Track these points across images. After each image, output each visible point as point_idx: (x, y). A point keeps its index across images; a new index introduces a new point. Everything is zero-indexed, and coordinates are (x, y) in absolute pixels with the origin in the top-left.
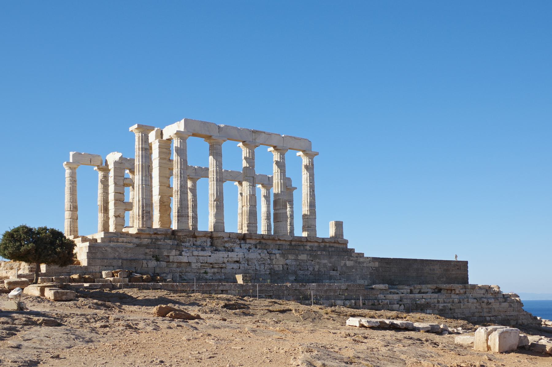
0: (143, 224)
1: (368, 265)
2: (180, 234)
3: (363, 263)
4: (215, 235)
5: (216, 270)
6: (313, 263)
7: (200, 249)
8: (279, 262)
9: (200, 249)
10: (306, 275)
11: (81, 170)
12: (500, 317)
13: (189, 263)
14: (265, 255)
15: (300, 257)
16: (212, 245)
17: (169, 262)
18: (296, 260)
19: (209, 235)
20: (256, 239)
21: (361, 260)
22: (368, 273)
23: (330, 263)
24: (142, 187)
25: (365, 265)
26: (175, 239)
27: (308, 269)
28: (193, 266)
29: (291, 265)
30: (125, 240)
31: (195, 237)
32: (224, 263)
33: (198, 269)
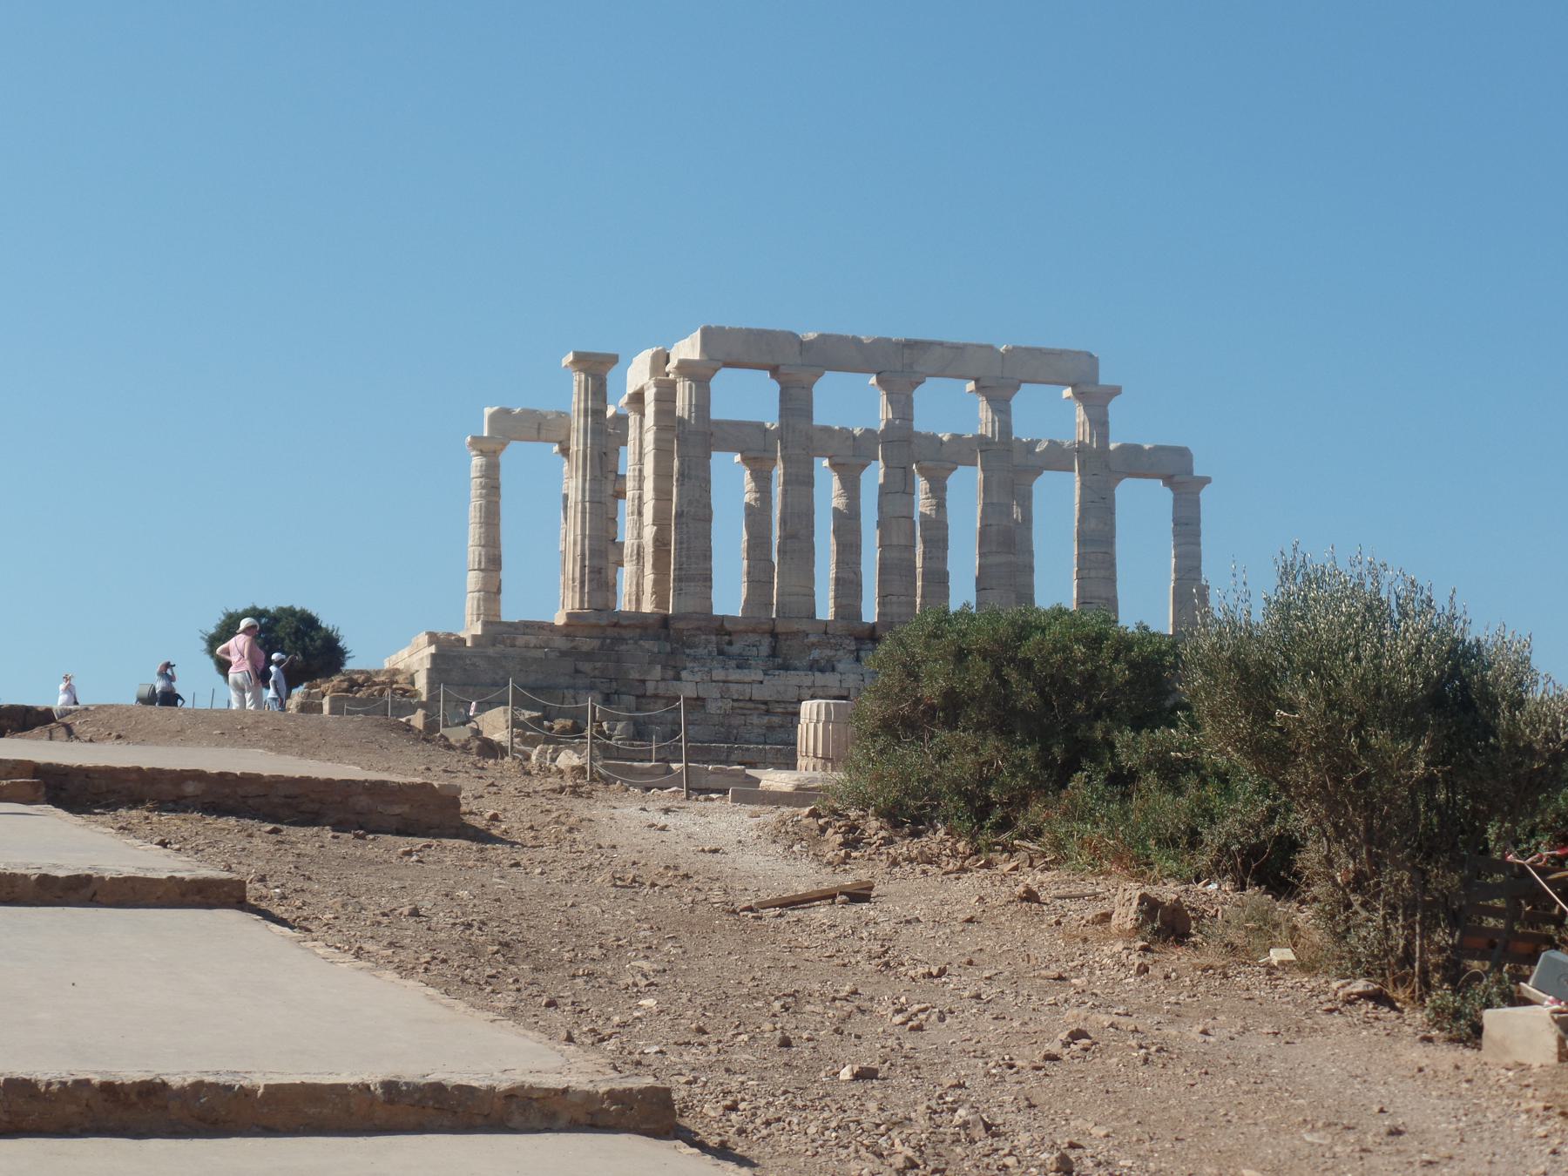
0: (582, 601)
2: (681, 625)
4: (780, 628)
5: (776, 720)
7: (733, 663)
9: (733, 663)
11: (515, 456)
16: (774, 653)
17: (644, 696)
19: (766, 627)
24: (584, 508)
26: (667, 638)
28: (712, 707)
30: (533, 640)
31: (729, 634)
33: (726, 715)
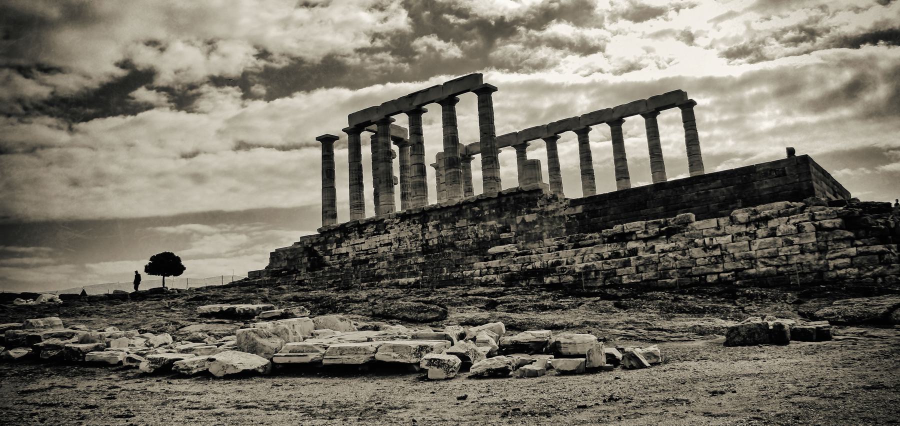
1: (561, 214)
3: (553, 212)
6: (476, 228)
8: (433, 236)
10: (467, 245)
12: (752, 271)
13: (347, 254)
14: (417, 228)
15: (457, 225)
18: (454, 229)
20: (416, 215)
21: (551, 208)
22: (563, 225)
23: (500, 223)
25: (557, 214)
27: (469, 238)
29: (447, 237)
32: (377, 247)
